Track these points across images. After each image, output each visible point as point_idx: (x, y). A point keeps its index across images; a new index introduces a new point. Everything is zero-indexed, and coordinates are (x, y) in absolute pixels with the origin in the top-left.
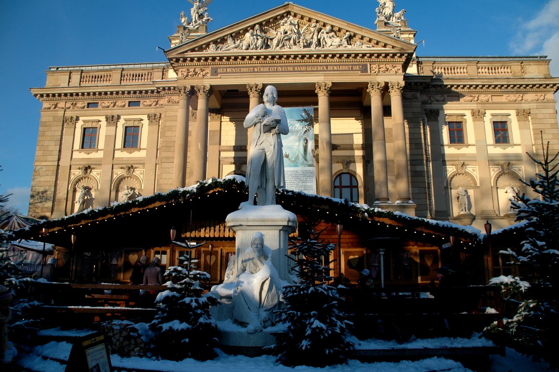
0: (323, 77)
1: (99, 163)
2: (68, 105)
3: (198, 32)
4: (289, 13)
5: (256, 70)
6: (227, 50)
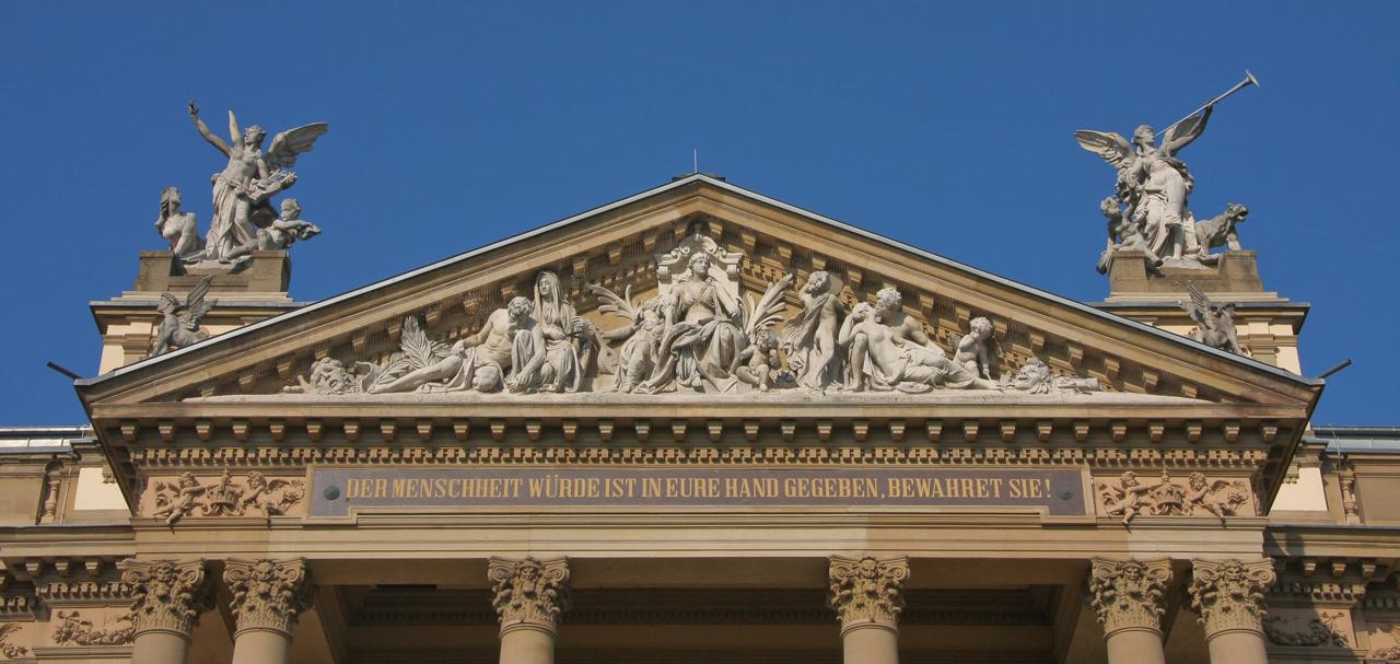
0: (862, 533)
3: (243, 287)
4: (698, 223)
5: (535, 488)
6: (397, 389)
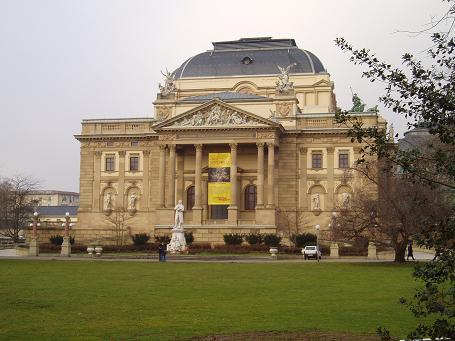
1: (116, 180)
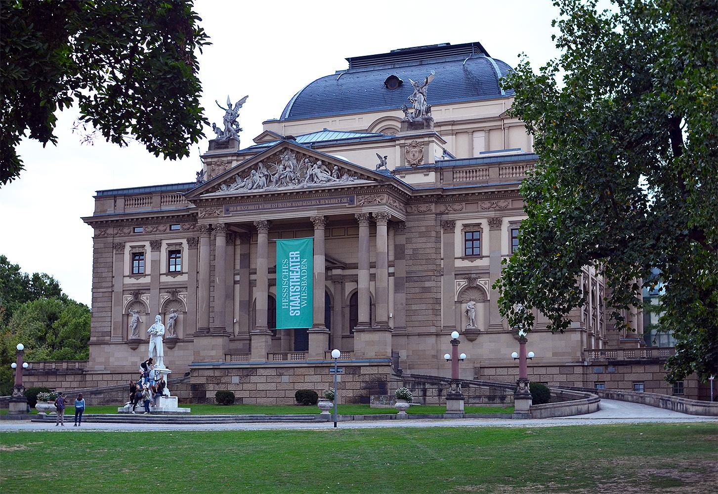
0: (316, 211)
1: (146, 289)
2: (116, 231)
